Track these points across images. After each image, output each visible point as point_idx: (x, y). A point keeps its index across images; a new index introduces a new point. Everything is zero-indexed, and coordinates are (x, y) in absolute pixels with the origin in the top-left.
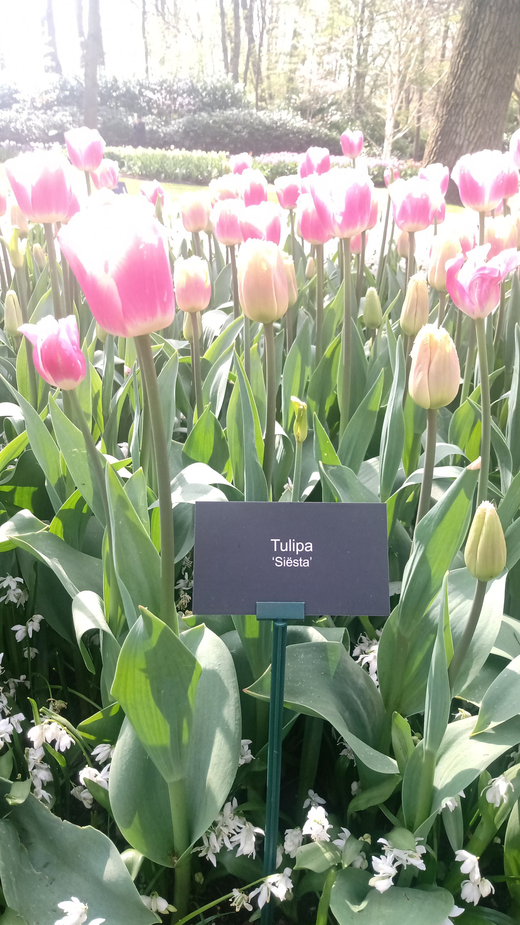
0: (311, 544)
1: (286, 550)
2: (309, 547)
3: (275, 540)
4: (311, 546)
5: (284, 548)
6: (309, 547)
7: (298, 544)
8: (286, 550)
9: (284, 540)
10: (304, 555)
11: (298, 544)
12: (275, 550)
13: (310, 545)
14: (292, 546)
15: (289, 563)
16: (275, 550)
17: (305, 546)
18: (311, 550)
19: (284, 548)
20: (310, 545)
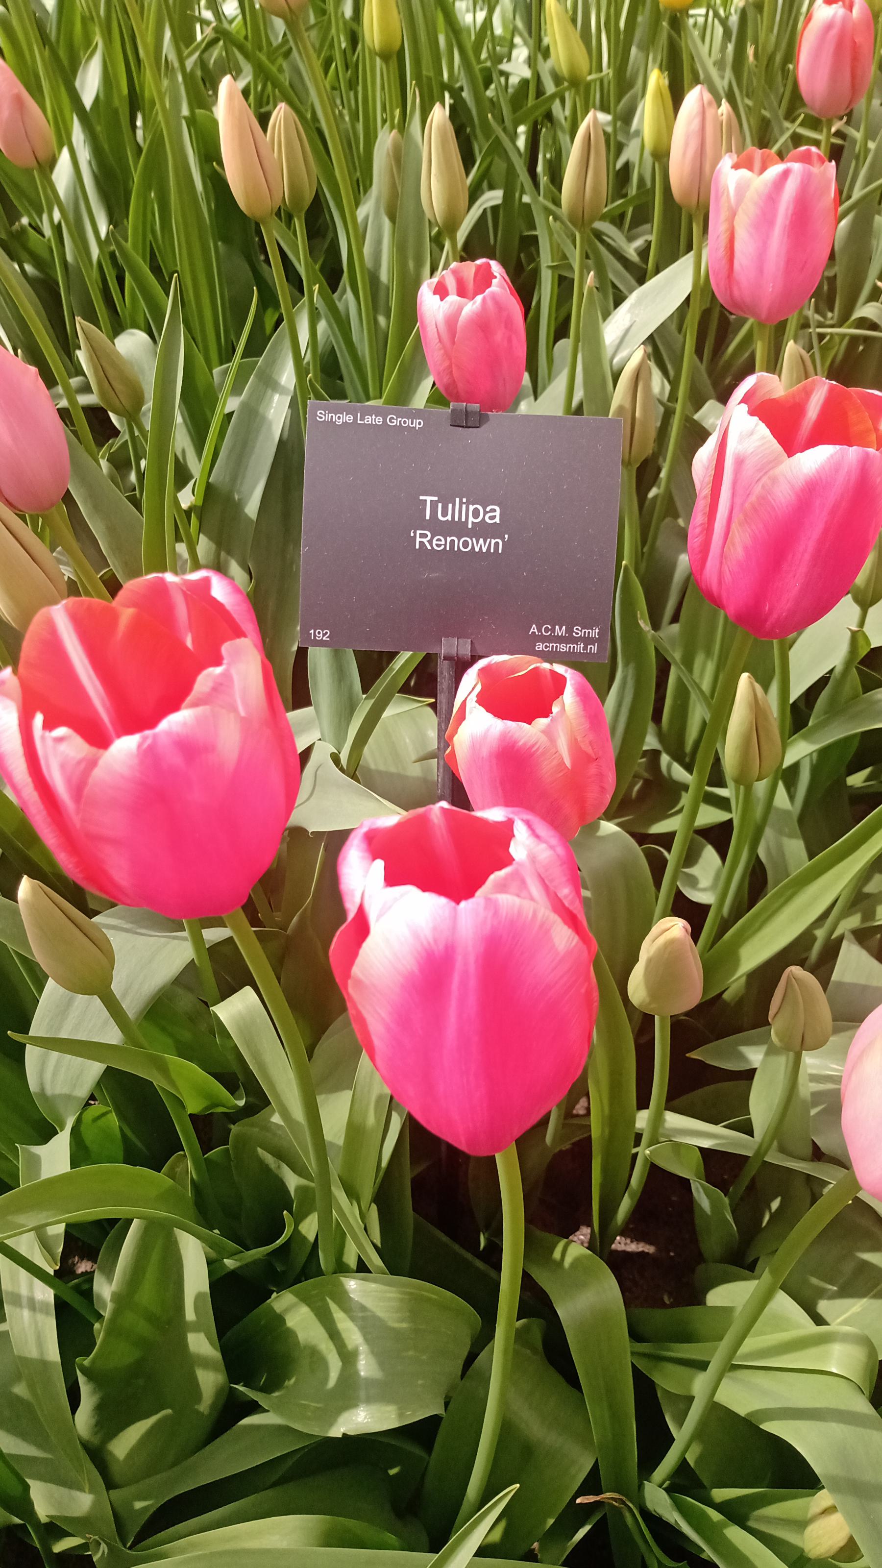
1: (449, 518)
2: (494, 514)
3: (429, 499)
4: (498, 514)
5: (445, 514)
6: (494, 514)
7: (471, 508)
8: (449, 518)
9: (446, 499)
10: (483, 531)
12: (428, 517)
13: (495, 511)
14: (461, 511)
16: (428, 517)
17: (485, 513)
18: (497, 520)
19: (445, 514)
20: (494, 510)
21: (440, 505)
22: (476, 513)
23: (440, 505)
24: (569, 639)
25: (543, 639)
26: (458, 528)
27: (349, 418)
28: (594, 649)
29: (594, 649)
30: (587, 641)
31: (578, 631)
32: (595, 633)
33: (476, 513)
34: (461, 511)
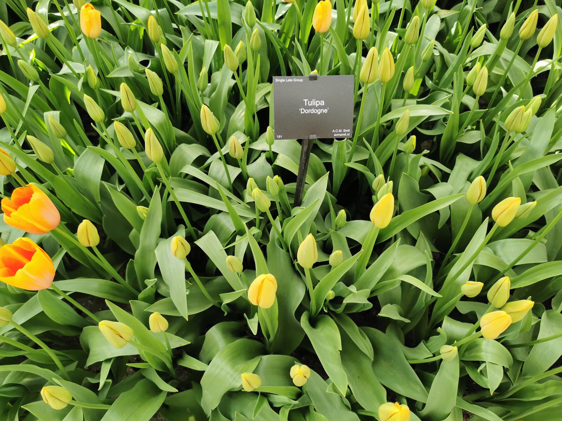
2: (322, 103)
3: (306, 100)
6: (322, 103)
9: (310, 100)
10: (320, 107)
22: (318, 103)
24: (343, 133)
25: (336, 133)
26: (314, 107)
27: (284, 81)
28: (349, 134)
29: (349, 134)
30: (347, 133)
31: (345, 131)
32: (349, 131)
33: (318, 103)
34: (314, 103)
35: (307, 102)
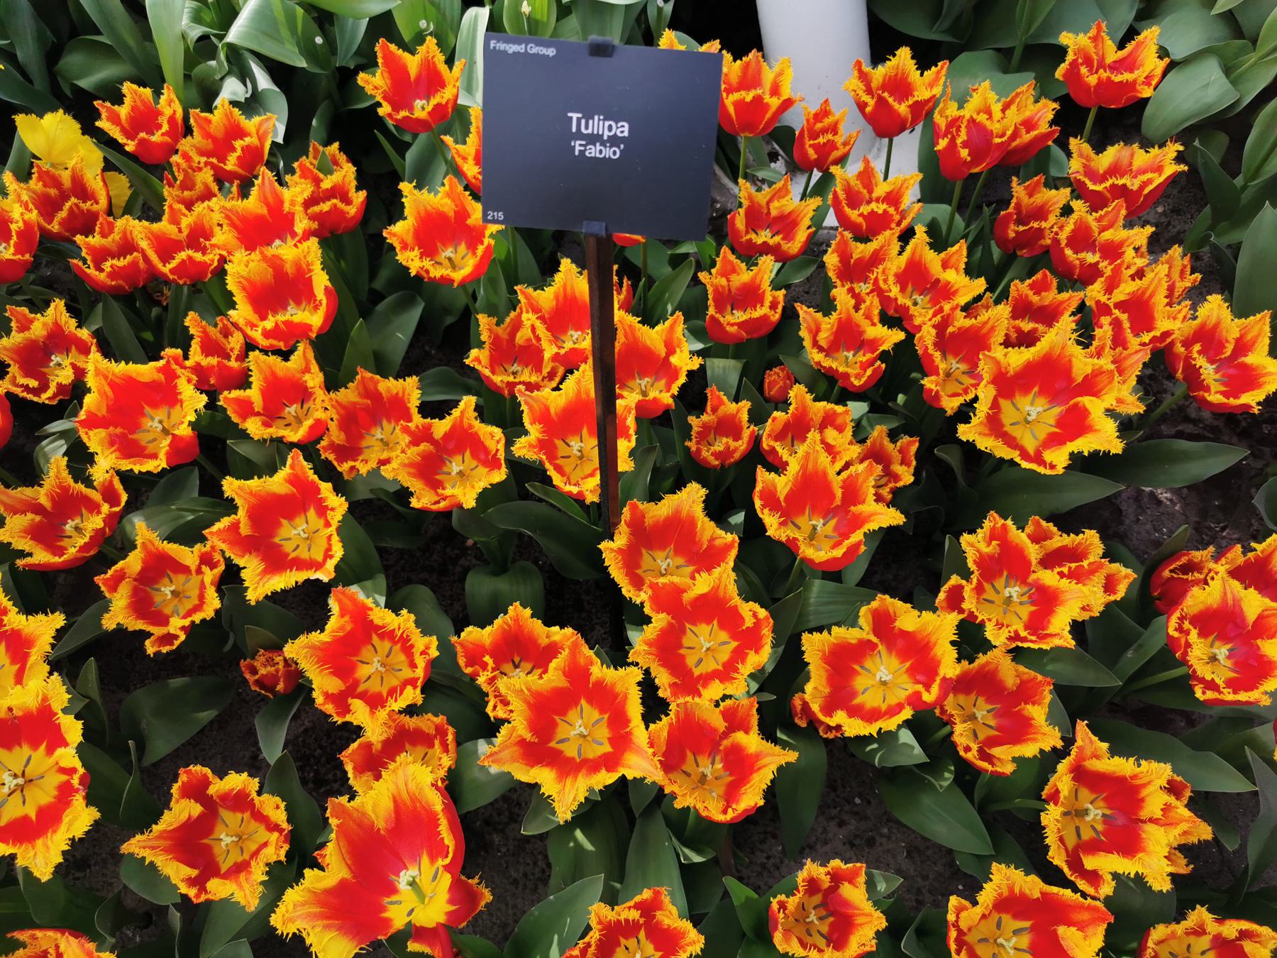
0: (626, 125)
2: (623, 129)
3: (575, 116)
4: (626, 129)
5: (587, 128)
6: (623, 129)
8: (590, 131)
9: (588, 116)
10: (614, 141)
11: (607, 123)
12: (574, 130)
14: (598, 125)
15: (593, 151)
16: (574, 130)
18: (626, 134)
19: (587, 128)
21: (583, 122)
22: (610, 128)
23: (583, 122)
26: (594, 139)
33: (610, 128)
35: (579, 120)
